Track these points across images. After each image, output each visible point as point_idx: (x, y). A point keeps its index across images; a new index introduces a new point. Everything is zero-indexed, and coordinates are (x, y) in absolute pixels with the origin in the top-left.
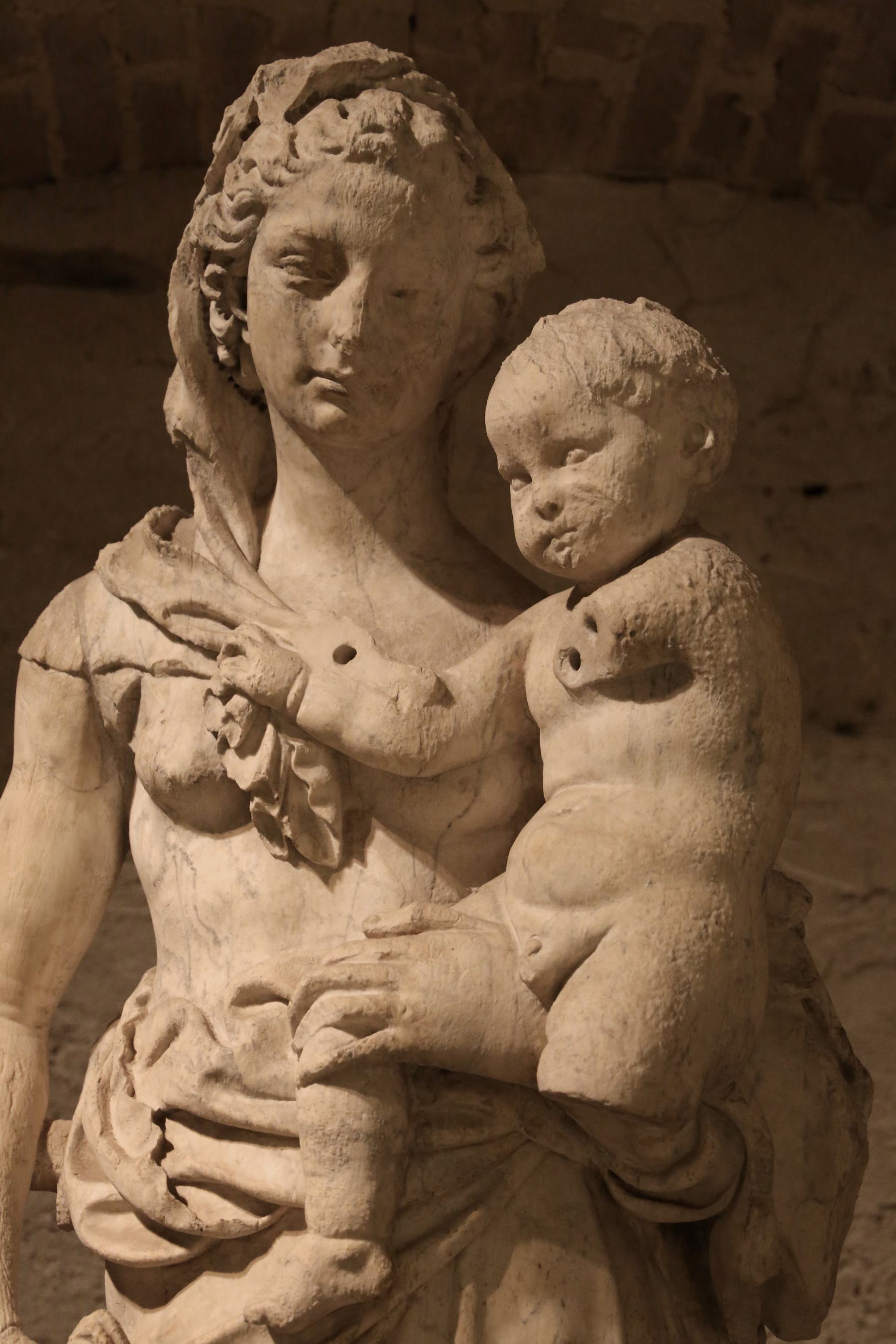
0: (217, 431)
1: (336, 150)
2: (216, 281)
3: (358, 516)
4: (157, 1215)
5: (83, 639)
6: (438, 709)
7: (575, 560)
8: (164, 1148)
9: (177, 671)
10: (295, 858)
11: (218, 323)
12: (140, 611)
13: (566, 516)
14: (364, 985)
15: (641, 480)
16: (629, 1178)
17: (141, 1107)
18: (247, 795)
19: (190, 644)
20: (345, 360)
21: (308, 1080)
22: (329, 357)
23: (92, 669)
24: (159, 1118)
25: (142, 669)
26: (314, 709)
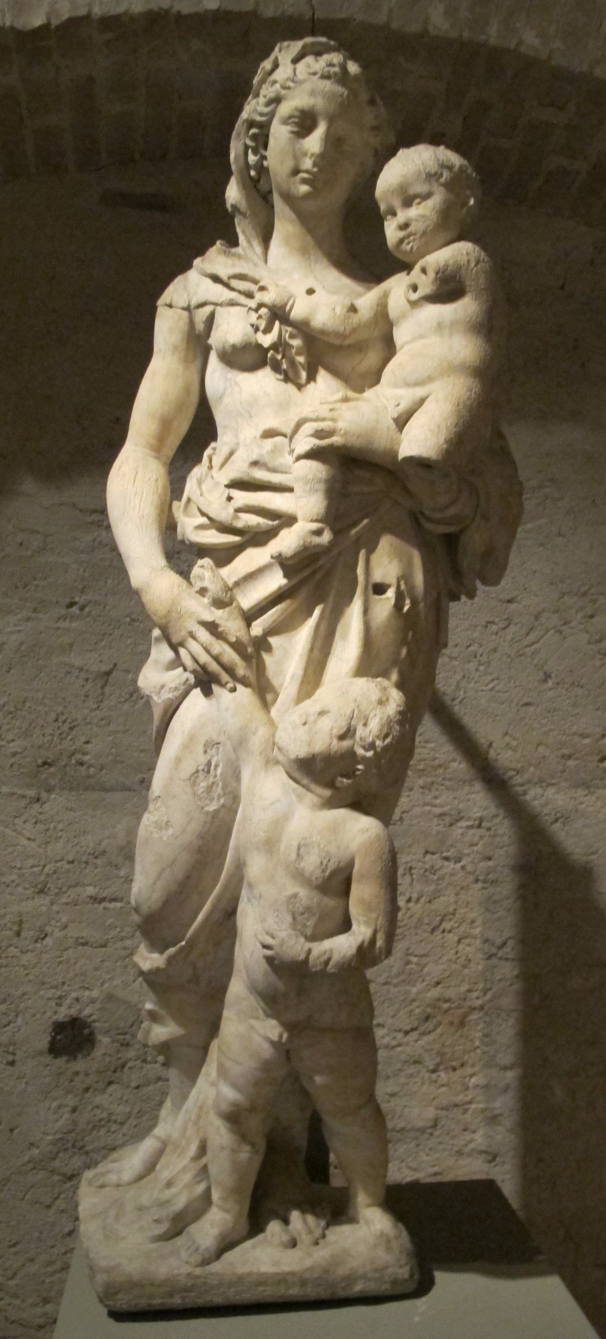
0: (250, 206)
1: (315, 74)
2: (254, 138)
3: (312, 242)
4: (230, 522)
6: (352, 314)
7: (415, 248)
8: (230, 499)
9: (232, 303)
10: (287, 379)
11: (252, 158)
12: (216, 279)
13: (412, 229)
14: (323, 420)
15: (445, 214)
16: (428, 513)
17: (218, 483)
18: (267, 350)
21: (299, 458)
22: (307, 164)
23: (192, 307)
24: (229, 486)
25: (216, 304)
26: (298, 312)
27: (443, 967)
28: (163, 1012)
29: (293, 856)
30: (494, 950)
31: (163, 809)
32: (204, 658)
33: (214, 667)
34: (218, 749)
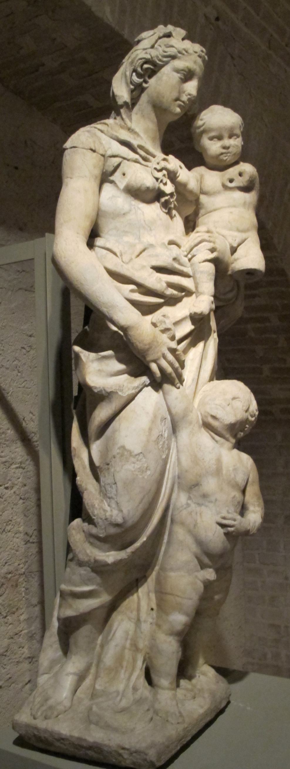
1: (196, 52)
5: (104, 147)
9: (136, 161)
19: (141, 156)
20: (189, 99)
22: (185, 98)
25: (124, 158)
27: (8, 553)
28: (102, 589)
29: (233, 476)
30: (28, 538)
31: (144, 460)
32: (169, 370)
33: (174, 375)
34: (165, 421)
